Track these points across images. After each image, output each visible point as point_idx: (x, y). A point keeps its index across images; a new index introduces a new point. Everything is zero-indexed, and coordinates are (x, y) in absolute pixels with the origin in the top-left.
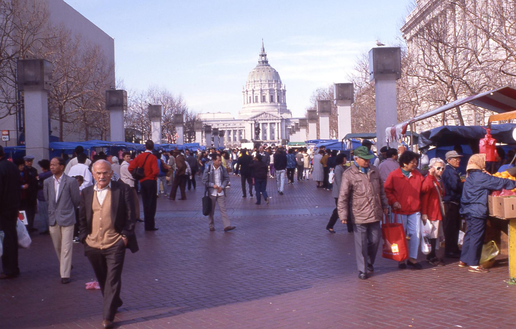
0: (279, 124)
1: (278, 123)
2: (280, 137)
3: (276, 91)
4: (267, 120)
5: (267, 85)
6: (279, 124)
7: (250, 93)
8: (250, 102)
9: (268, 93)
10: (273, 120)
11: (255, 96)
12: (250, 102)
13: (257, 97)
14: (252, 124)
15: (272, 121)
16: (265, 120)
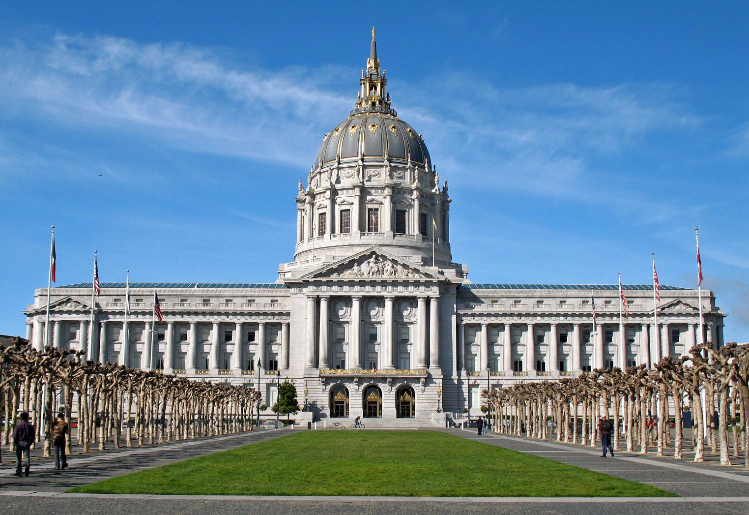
0: (433, 305)
1: (427, 301)
2: (433, 357)
3: (415, 194)
4: (384, 284)
5: (384, 173)
6: (433, 305)
7: (324, 201)
8: (322, 233)
9: (387, 202)
10: (406, 284)
11: (338, 209)
12: (322, 233)
13: (345, 213)
14: (317, 300)
15: (401, 291)
16: (373, 284)
